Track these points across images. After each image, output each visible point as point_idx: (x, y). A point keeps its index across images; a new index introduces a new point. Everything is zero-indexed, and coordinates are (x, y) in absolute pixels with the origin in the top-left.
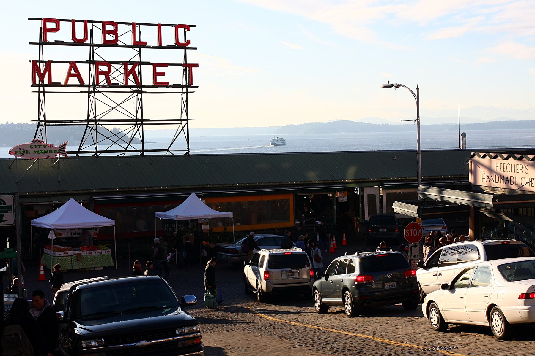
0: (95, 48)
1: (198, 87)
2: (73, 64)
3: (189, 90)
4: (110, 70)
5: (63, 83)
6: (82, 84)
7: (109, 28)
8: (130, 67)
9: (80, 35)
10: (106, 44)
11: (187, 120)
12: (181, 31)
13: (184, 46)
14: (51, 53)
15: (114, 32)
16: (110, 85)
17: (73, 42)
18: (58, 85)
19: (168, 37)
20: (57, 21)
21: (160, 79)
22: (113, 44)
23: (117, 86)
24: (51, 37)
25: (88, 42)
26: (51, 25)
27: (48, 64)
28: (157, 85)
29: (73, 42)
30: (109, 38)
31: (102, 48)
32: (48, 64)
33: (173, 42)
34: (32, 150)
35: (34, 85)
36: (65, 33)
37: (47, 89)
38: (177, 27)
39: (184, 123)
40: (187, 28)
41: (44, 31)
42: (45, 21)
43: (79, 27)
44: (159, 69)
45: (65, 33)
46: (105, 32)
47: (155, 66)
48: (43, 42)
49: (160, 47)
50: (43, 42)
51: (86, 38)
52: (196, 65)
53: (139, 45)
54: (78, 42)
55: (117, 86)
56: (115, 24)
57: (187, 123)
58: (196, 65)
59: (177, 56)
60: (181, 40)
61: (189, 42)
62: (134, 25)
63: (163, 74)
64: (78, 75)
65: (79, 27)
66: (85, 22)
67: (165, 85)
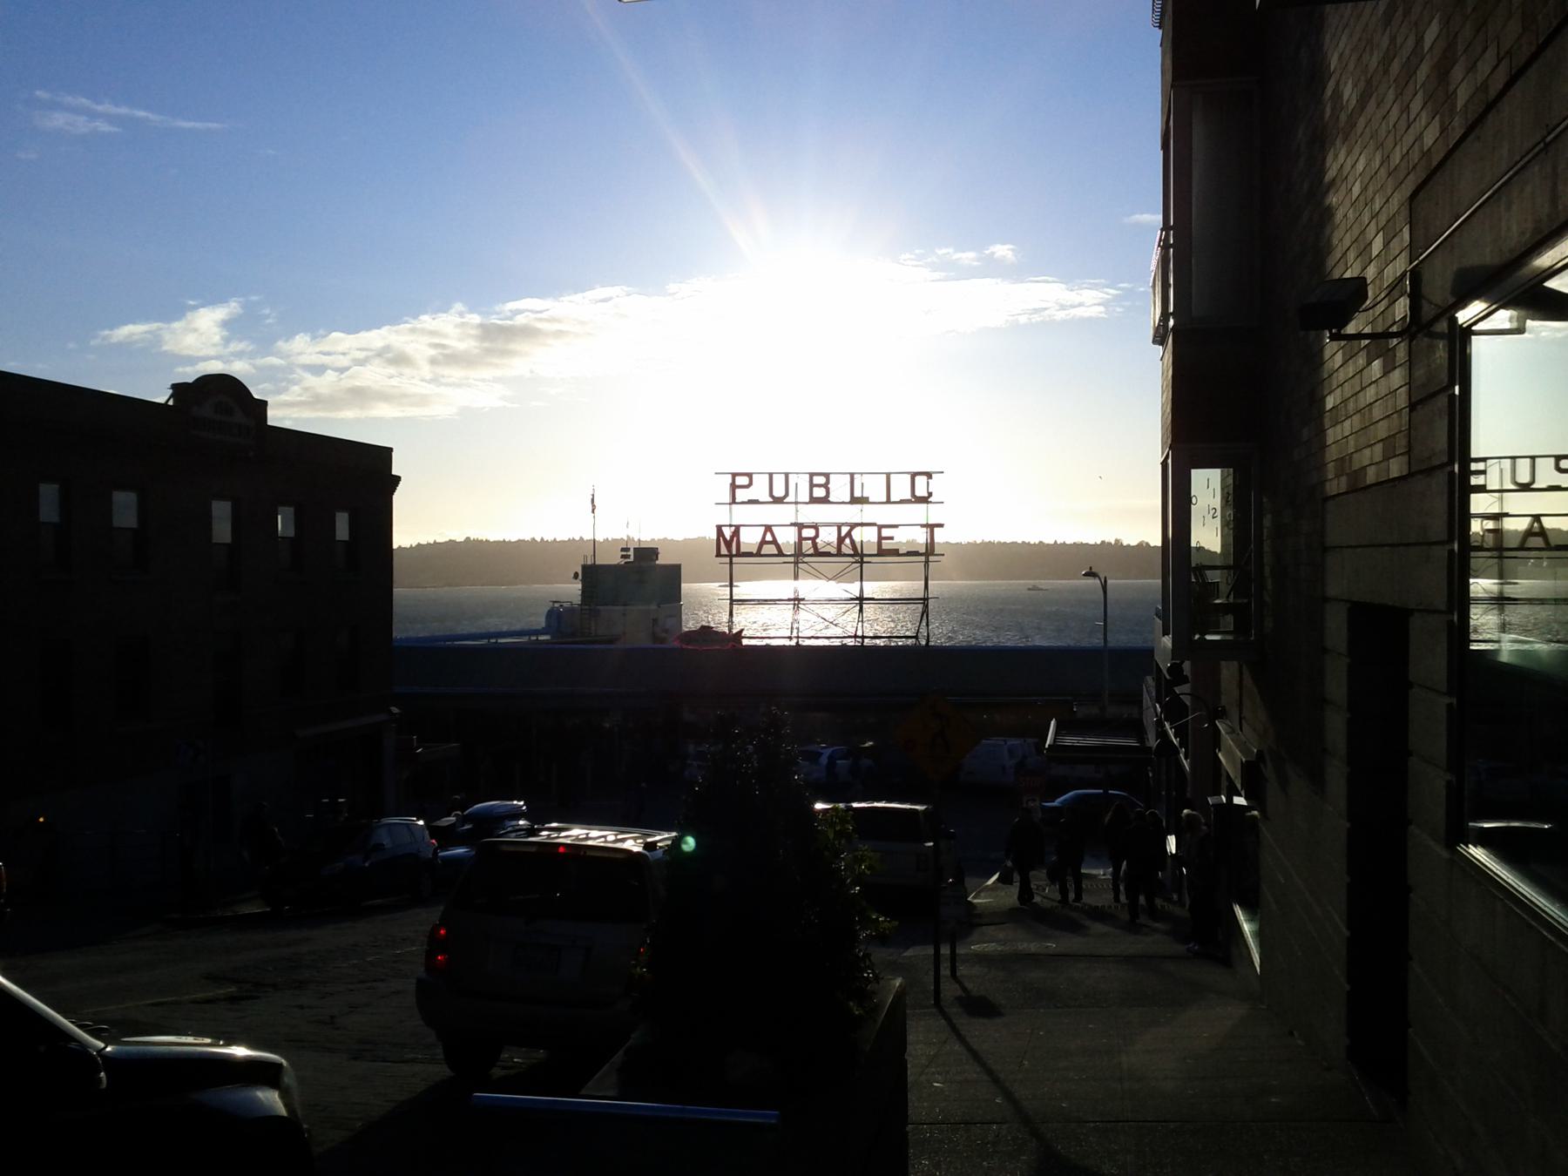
2: (768, 528)
4: (817, 535)
6: (781, 554)
7: (821, 480)
8: (845, 530)
9: (779, 491)
10: (814, 500)
12: (921, 480)
13: (924, 500)
14: (741, 515)
15: (826, 486)
19: (901, 489)
20: (750, 475)
21: (886, 545)
22: (825, 500)
23: (828, 554)
24: (741, 495)
25: (790, 498)
26: (741, 481)
27: (738, 528)
30: (819, 493)
32: (738, 528)
33: (908, 496)
35: (719, 555)
36: (760, 490)
37: (735, 560)
38: (914, 475)
40: (929, 475)
41: (734, 487)
42: (734, 475)
43: (779, 482)
44: (885, 532)
45: (760, 490)
46: (812, 486)
47: (880, 527)
48: (734, 501)
49: (888, 501)
50: (734, 501)
51: (787, 494)
52: (941, 526)
54: (778, 501)
55: (828, 554)
56: (827, 475)
58: (941, 526)
59: (918, 513)
60: (921, 491)
61: (930, 494)
62: (852, 475)
64: (774, 542)
65: (779, 482)
66: (787, 475)
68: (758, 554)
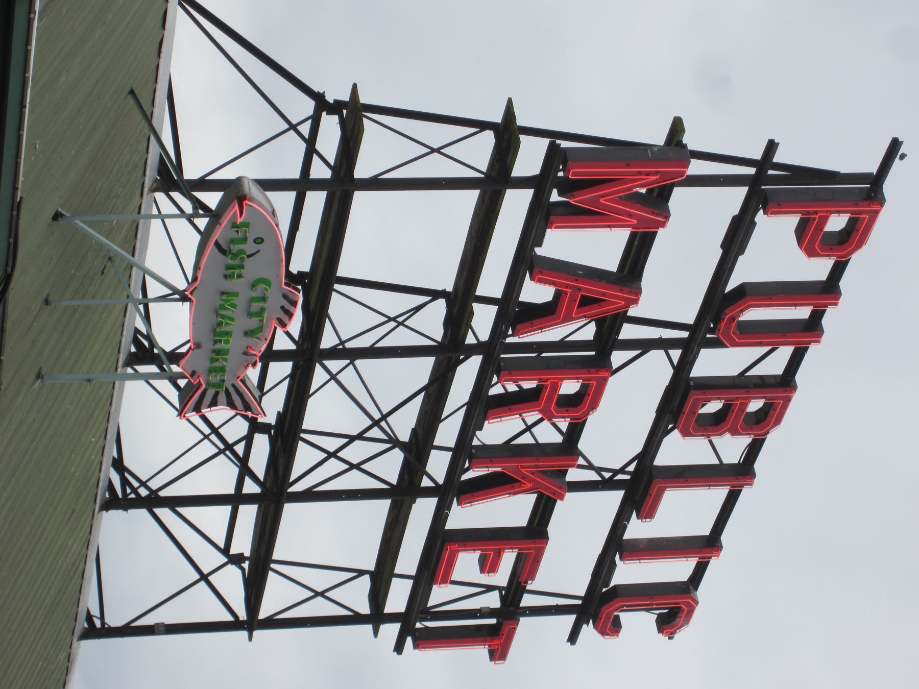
0: (676, 354)
1: (399, 648)
3: (391, 630)
5: (539, 251)
11: (252, 623)
16: (481, 407)
17: (732, 285)
18: (532, 234)
28: (441, 545)
29: (733, 283)
31: (665, 374)
34: (235, 285)
39: (231, 581)
49: (616, 546)
52: (498, 654)
53: (642, 485)
57: (235, 625)
63: (488, 565)
67: (433, 566)
68: (526, 262)
